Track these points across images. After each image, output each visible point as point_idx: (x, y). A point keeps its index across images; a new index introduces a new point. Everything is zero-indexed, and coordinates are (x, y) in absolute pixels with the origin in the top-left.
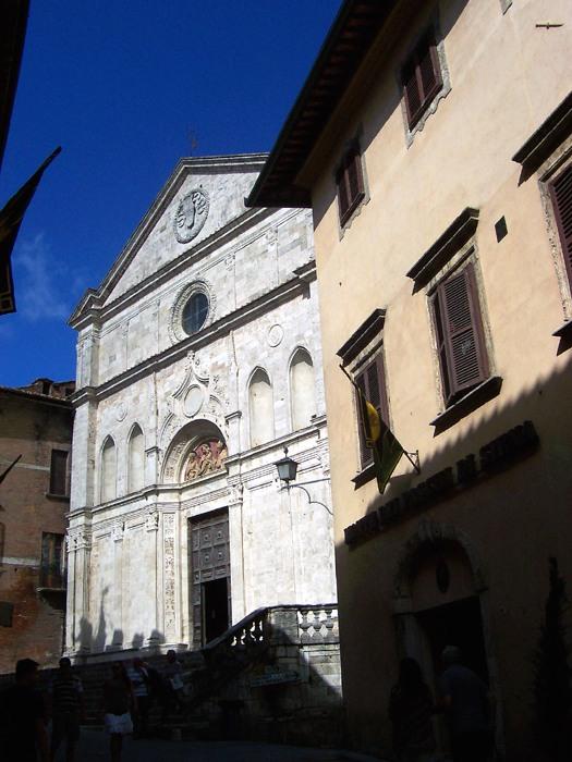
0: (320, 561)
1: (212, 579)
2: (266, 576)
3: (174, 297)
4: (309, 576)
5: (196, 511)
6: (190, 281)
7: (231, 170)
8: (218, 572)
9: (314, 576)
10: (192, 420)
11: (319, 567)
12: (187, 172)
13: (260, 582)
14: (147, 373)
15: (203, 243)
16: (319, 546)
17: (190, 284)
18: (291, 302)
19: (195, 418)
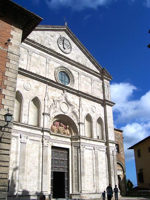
0: (104, 176)
1: (58, 171)
2: (90, 176)
3: (58, 65)
4: (102, 179)
5: (56, 145)
6: (66, 67)
7: (81, 49)
8: (61, 169)
9: (103, 180)
10: (64, 114)
11: (104, 177)
12: (65, 30)
13: (88, 178)
14: (45, 82)
15: (65, 57)
16: (104, 172)
17: (65, 67)
18: (98, 104)
19: (65, 114)
